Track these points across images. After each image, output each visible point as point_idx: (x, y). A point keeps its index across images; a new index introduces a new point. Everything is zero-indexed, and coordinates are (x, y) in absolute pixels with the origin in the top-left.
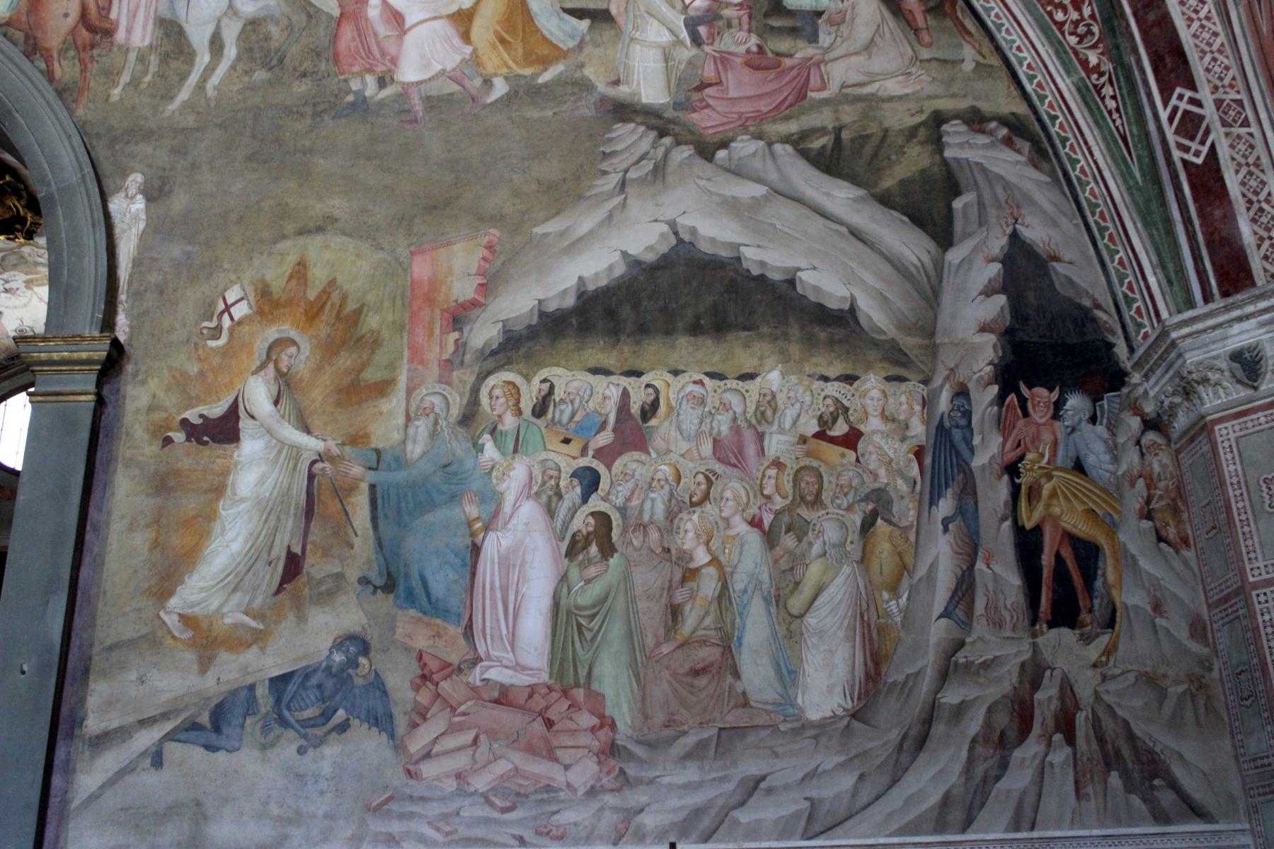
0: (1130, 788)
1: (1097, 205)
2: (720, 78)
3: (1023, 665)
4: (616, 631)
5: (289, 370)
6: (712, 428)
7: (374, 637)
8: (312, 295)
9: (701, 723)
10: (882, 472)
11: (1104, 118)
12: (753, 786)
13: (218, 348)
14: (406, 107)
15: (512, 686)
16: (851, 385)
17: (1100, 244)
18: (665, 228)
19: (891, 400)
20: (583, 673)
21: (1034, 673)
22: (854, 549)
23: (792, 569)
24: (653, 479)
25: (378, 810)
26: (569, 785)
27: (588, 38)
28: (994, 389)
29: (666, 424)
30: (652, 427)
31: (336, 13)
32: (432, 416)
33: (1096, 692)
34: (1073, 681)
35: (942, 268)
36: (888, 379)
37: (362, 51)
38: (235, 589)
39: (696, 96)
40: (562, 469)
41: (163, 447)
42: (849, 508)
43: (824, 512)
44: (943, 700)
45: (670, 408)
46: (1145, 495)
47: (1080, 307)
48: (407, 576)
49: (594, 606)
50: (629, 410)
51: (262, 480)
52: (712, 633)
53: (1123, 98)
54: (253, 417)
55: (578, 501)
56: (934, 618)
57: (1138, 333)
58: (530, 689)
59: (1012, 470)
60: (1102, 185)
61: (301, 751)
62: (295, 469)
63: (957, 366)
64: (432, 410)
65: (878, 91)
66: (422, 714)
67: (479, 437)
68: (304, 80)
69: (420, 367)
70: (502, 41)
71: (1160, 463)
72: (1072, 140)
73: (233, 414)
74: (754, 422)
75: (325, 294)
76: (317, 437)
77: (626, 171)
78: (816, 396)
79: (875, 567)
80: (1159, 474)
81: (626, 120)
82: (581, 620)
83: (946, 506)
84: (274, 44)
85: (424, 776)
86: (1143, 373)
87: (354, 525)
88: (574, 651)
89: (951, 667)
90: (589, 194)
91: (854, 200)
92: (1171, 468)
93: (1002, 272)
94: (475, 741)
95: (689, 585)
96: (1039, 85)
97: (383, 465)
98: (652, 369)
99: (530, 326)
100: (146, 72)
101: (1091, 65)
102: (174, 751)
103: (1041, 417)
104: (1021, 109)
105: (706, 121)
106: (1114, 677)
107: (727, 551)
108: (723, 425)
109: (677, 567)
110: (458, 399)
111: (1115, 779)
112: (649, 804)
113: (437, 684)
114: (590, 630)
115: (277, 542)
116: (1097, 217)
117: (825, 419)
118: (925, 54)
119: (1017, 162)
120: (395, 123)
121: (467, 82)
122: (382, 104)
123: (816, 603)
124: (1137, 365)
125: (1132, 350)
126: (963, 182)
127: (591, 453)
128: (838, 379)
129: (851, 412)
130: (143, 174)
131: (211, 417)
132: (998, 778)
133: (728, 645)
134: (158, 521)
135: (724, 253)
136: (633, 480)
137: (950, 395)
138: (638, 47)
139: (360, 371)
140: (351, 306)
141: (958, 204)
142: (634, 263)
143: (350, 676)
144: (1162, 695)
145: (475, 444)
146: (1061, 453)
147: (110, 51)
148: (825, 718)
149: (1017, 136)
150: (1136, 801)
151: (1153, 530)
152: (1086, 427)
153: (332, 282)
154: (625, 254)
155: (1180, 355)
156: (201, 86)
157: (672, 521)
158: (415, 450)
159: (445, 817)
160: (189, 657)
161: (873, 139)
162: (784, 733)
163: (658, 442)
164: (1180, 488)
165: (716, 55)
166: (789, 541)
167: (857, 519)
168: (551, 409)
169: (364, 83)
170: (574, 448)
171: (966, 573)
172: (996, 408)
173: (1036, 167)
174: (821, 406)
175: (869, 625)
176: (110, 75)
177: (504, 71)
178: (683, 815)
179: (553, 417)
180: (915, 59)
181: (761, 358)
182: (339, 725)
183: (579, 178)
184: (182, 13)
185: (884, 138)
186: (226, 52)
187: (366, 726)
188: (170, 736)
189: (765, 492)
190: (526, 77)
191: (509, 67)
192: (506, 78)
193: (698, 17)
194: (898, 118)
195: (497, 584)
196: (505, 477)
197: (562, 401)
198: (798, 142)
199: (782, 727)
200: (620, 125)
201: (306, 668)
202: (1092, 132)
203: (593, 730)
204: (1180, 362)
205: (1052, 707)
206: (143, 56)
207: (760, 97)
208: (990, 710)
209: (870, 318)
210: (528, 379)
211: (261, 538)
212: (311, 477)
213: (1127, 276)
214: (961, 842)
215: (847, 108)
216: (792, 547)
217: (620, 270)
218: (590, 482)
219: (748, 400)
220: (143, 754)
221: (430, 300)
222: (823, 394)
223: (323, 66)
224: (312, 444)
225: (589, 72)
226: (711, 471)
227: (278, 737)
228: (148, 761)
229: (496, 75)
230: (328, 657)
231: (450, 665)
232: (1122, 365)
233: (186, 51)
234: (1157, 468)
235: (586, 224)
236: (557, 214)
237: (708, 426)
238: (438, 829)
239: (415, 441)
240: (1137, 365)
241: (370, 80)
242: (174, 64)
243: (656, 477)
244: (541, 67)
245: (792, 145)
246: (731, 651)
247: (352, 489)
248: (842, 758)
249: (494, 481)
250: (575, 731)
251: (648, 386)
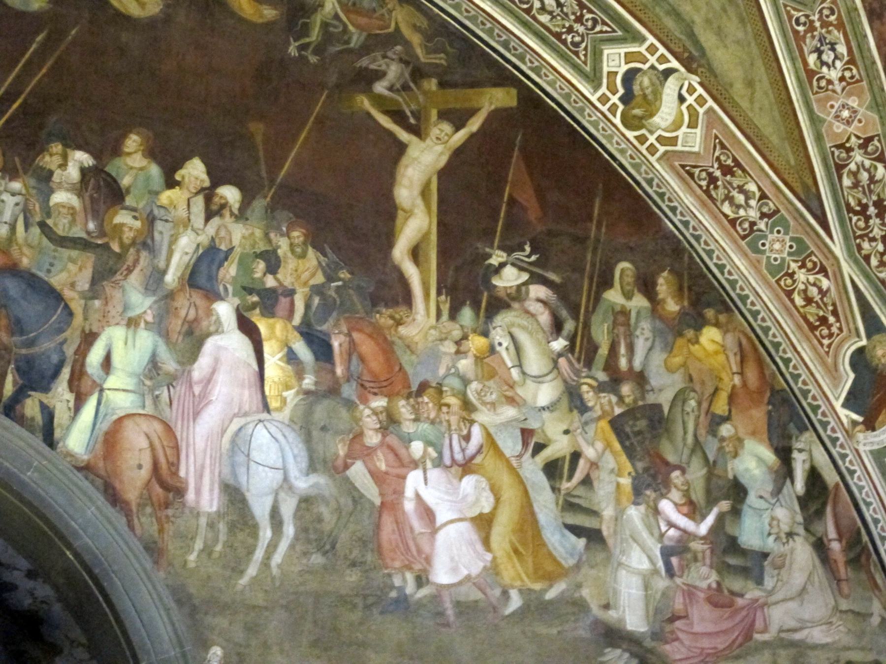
2: (687, 612)
14: (440, 609)
27: (584, 558)
31: (378, 501)
37: (401, 545)
39: (668, 628)
68: (354, 569)
70: (516, 551)
81: (614, 645)
84: (327, 527)
100: (216, 540)
118: (844, 605)
120: (431, 623)
121: (488, 590)
122: (420, 604)
130: (223, 648)
138: (624, 572)
147: (183, 513)
165: (685, 588)
169: (404, 580)
176: (188, 538)
177: (518, 583)
180: (836, 609)
184: (243, 479)
191: (522, 581)
192: (521, 591)
193: (672, 547)
200: (609, 650)
206: (213, 523)
207: (717, 634)
215: (783, 653)
223: (369, 557)
225: (585, 593)
229: (513, 587)
233: (250, 522)
241: (410, 577)
242: (241, 536)
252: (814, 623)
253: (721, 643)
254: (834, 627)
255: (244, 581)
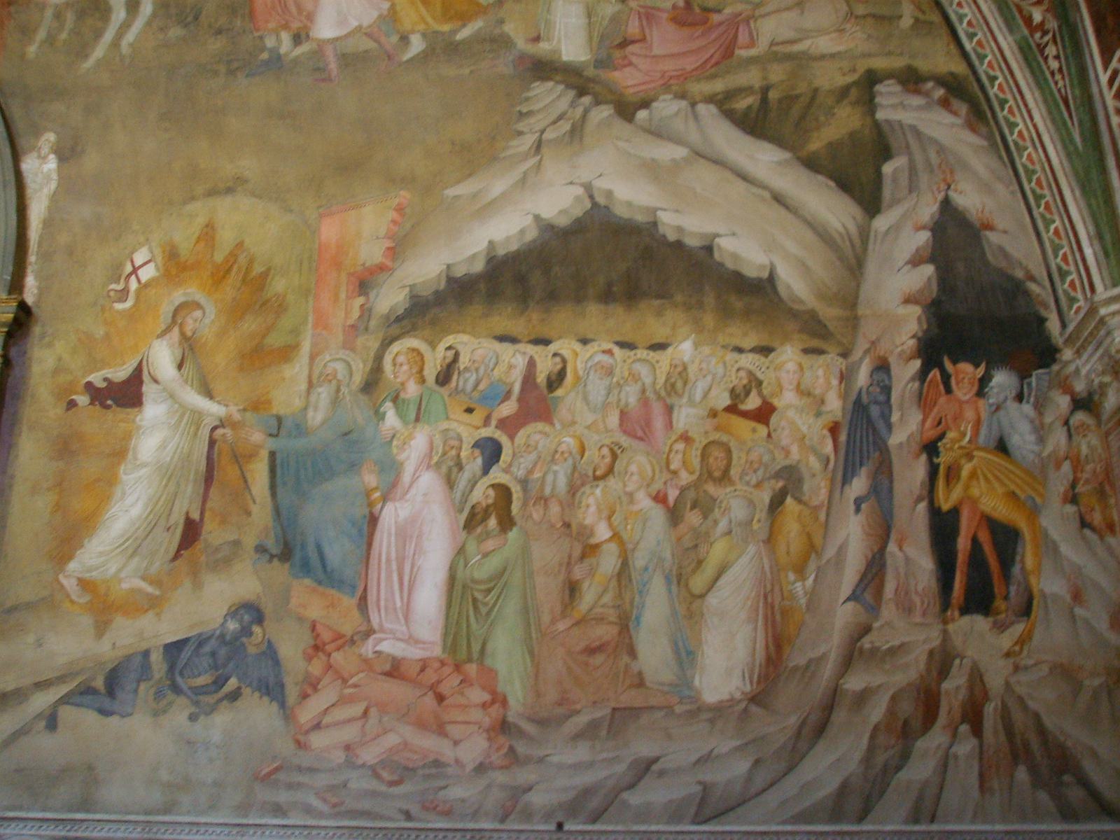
0: (1037, 781)
1: (1034, 172)
2: (644, 35)
3: (931, 653)
4: (511, 608)
5: (194, 333)
6: (619, 400)
7: (268, 608)
8: (219, 257)
9: (595, 703)
10: (795, 449)
11: (1045, 79)
12: (644, 768)
13: (124, 311)
15: (404, 659)
16: (766, 357)
17: (1035, 213)
18: (580, 191)
19: (808, 374)
20: (476, 648)
21: (942, 661)
22: (760, 526)
23: (696, 546)
24: (556, 452)
25: (267, 779)
26: (457, 761)
28: (917, 364)
29: (573, 394)
30: (559, 397)
32: (334, 382)
33: (1007, 684)
34: (983, 670)
35: (868, 237)
36: (806, 351)
38: (132, 556)
39: (617, 54)
40: (464, 439)
41: (68, 409)
42: (758, 485)
43: (732, 489)
44: (846, 686)
45: (577, 378)
46: (1071, 477)
47: (1011, 279)
48: (303, 546)
49: (490, 580)
50: (535, 379)
51: (163, 446)
52: (611, 611)
53: (1066, 58)
54: (156, 381)
55: (478, 471)
56: (842, 600)
57: (1070, 307)
58: (421, 663)
59: (931, 448)
60: (1040, 150)
61: (193, 718)
62: (196, 434)
63: (878, 339)
64: (335, 376)
65: (810, 47)
66: (311, 686)
67: (380, 406)
68: (219, 37)
69: (324, 332)
71: (1088, 444)
72: (1011, 102)
73: (136, 378)
74: (663, 393)
75: (233, 256)
76: (219, 403)
77: (542, 132)
78: (729, 368)
79: (781, 549)
80: (1086, 456)
81: (544, 79)
82: (478, 595)
83: (859, 485)
85: (313, 748)
86: (1075, 349)
87: (254, 493)
88: (468, 626)
89: (856, 653)
90: (503, 155)
91: (779, 163)
92: (1100, 450)
93: (931, 238)
94: (366, 713)
95: (587, 562)
96: (979, 43)
97: (283, 432)
98: (560, 338)
99: (437, 292)
100: (61, 28)
101: (1034, 24)
102: (66, 713)
103: (965, 394)
104: (959, 68)
105: (628, 80)
106: (1026, 668)
107: (629, 527)
108: (631, 396)
109: (576, 543)
110: (361, 366)
111: (1022, 774)
112: (537, 783)
113: (329, 655)
114: (486, 604)
115: (176, 508)
116: (1033, 184)
117: (738, 392)
119: (953, 125)
121: (383, 40)
122: (296, 61)
123: (718, 584)
124: (1069, 341)
125: (1064, 325)
126: (894, 144)
127: (494, 423)
128: (753, 350)
129: (765, 384)
130: (55, 132)
131: (117, 380)
132: (899, 768)
133: (626, 623)
134: (60, 484)
135: (640, 218)
136: (535, 452)
137: (871, 369)
139: (264, 337)
140: (258, 269)
141: (887, 169)
142: (547, 228)
143: (243, 645)
144: (1077, 687)
145: (377, 412)
146: (983, 432)
148: (722, 702)
149: (956, 96)
150: (1043, 796)
151: (1077, 515)
152: (1012, 406)
153: (240, 245)
154: (537, 218)
155: (1108, 333)
156: (116, 44)
157: (574, 494)
158: (316, 417)
159: (332, 788)
160: (87, 621)
161: (802, 99)
162: (679, 716)
163: (563, 413)
164: (1108, 471)
165: (642, 10)
166: (693, 518)
167: (767, 499)
168: (455, 377)
169: (279, 40)
170: (477, 417)
171: (877, 556)
172: (917, 384)
173: (973, 130)
174: (734, 378)
175: (773, 608)
177: (422, 27)
178: (570, 795)
179: (457, 385)
180: (851, 14)
181: (674, 328)
182: (231, 693)
183: (494, 138)
185: (813, 98)
186: (142, 9)
187: (257, 694)
188: (64, 700)
189: (672, 467)
190: (443, 34)
191: (427, 23)
192: (424, 35)
194: (829, 78)
195: (393, 555)
196: (406, 447)
197: (466, 369)
198: (722, 102)
199: (678, 709)
200: (537, 84)
201: (200, 635)
202: (1033, 94)
203: (484, 706)
204: (1108, 340)
205: (960, 697)
208: (893, 698)
209: (789, 287)
210: (433, 345)
211: (161, 503)
212: (212, 443)
213: (1062, 247)
214: (857, 833)
216: (697, 525)
217: (532, 235)
218: (491, 452)
219: (658, 372)
220: (39, 716)
221: (338, 265)
222: (737, 366)
223: (238, 23)
224: (214, 409)
225: (509, 28)
226: (617, 444)
227: (170, 704)
228: (43, 724)
229: (413, 32)
230: (222, 625)
231: (344, 636)
232: (1054, 341)
234: (1084, 450)
235: (498, 186)
236: (470, 175)
237: (616, 397)
238: (324, 800)
239: (316, 409)
240: (1069, 341)
241: (286, 37)
243: (560, 450)
244: (460, 23)
245: (716, 105)
246: (628, 630)
247: (252, 456)
248: (738, 743)
249: (395, 451)
250: (466, 707)
251: (555, 355)
252: (821, 32)
253: (690, 64)
254: (848, 34)
255: (89, 63)
